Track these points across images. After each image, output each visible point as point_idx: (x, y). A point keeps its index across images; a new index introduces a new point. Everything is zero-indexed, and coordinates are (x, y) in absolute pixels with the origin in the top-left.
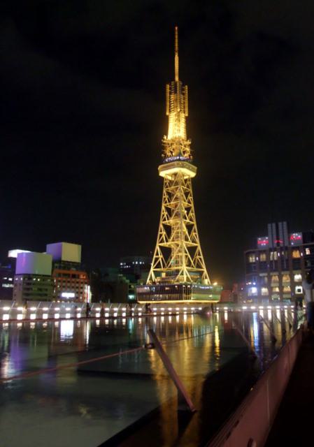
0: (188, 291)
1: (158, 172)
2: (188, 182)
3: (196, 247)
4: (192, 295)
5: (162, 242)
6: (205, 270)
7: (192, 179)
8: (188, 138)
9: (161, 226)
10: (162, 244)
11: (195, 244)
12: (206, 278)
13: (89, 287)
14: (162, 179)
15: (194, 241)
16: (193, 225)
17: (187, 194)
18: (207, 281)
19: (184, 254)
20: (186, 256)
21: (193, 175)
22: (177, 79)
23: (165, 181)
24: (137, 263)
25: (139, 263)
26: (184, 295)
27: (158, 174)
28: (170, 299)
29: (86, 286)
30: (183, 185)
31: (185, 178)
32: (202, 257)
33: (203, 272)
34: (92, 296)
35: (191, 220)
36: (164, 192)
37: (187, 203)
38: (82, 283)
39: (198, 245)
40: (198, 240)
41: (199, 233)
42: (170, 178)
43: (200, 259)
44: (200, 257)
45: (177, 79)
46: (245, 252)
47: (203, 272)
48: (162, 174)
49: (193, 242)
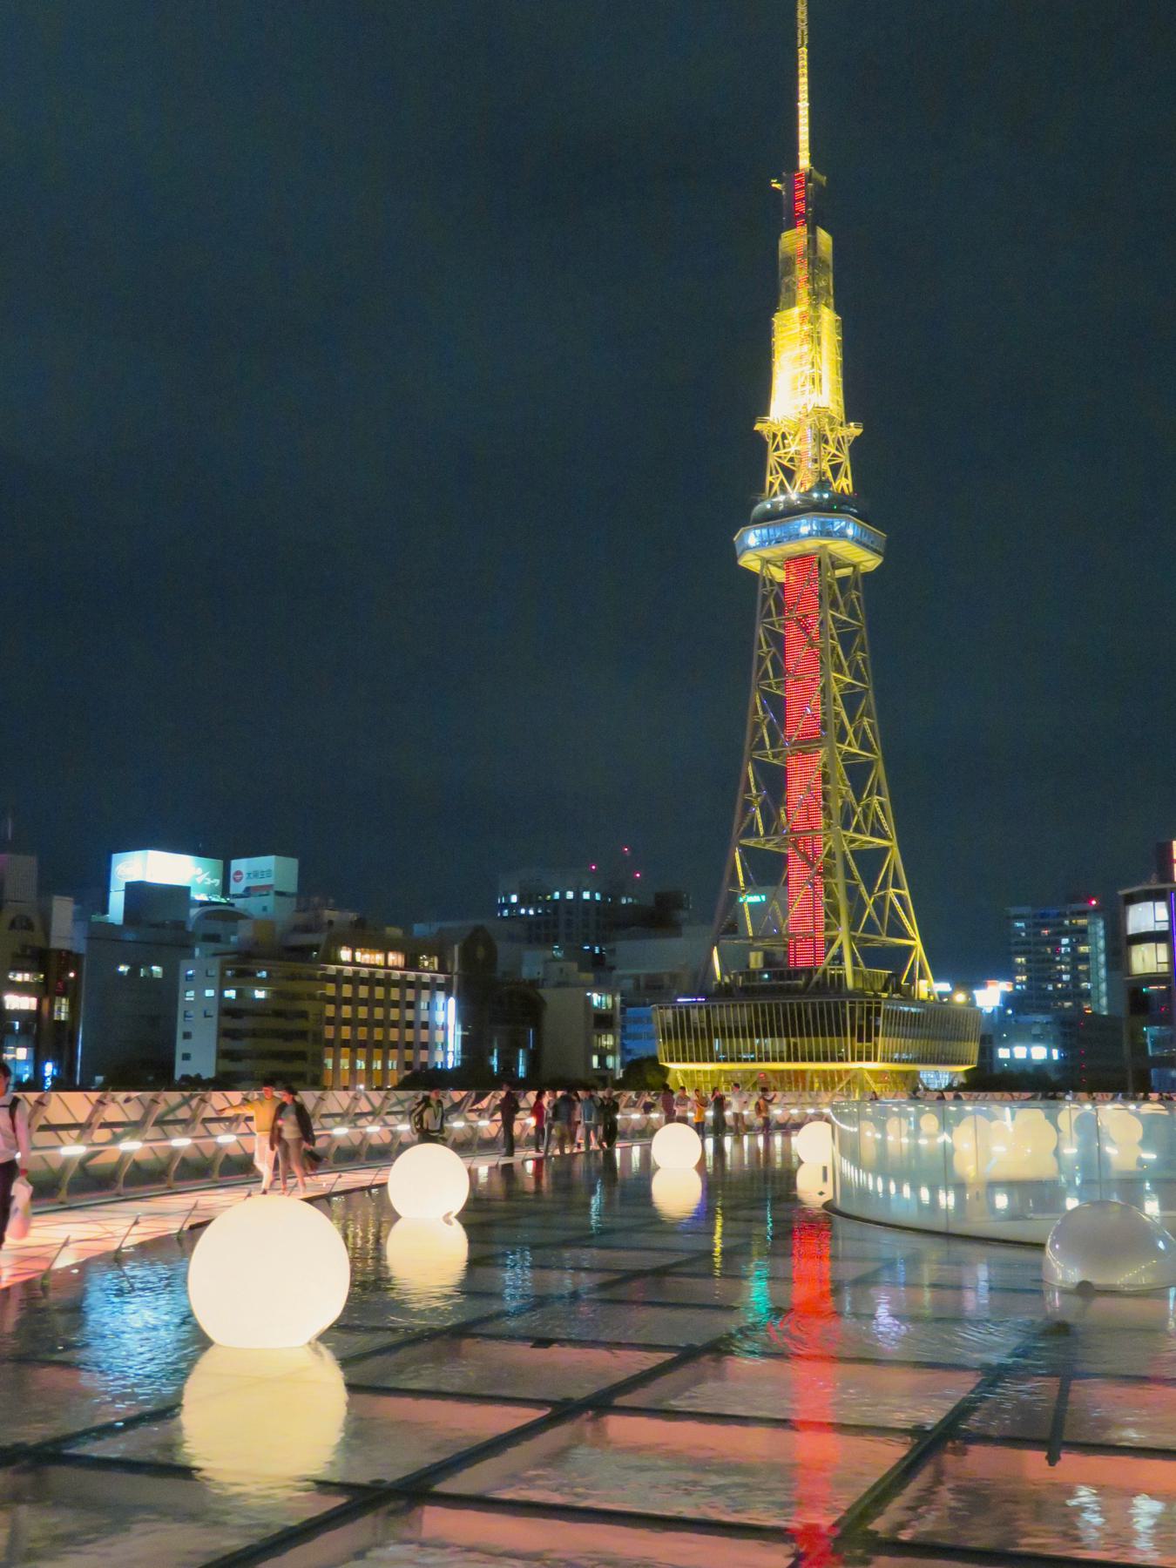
3: (886, 850)
5: (751, 831)
6: (917, 943)
7: (866, 575)
8: (851, 413)
10: (751, 842)
11: (885, 843)
12: (922, 976)
13: (452, 1001)
14: (751, 577)
16: (869, 766)
17: (846, 640)
20: (852, 892)
21: (870, 561)
22: (804, 162)
23: (761, 591)
24: (586, 895)
25: (592, 896)
27: (735, 559)
28: (793, 1056)
29: (440, 997)
30: (834, 604)
31: (840, 573)
32: (906, 893)
33: (908, 950)
34: (463, 1037)
35: (865, 745)
36: (760, 632)
38: (426, 986)
39: (892, 844)
40: (888, 826)
41: (892, 799)
42: (779, 575)
43: (899, 897)
44: (898, 894)
45: (804, 162)
46: (1122, 893)
47: (908, 950)
48: (750, 562)
49: (872, 835)
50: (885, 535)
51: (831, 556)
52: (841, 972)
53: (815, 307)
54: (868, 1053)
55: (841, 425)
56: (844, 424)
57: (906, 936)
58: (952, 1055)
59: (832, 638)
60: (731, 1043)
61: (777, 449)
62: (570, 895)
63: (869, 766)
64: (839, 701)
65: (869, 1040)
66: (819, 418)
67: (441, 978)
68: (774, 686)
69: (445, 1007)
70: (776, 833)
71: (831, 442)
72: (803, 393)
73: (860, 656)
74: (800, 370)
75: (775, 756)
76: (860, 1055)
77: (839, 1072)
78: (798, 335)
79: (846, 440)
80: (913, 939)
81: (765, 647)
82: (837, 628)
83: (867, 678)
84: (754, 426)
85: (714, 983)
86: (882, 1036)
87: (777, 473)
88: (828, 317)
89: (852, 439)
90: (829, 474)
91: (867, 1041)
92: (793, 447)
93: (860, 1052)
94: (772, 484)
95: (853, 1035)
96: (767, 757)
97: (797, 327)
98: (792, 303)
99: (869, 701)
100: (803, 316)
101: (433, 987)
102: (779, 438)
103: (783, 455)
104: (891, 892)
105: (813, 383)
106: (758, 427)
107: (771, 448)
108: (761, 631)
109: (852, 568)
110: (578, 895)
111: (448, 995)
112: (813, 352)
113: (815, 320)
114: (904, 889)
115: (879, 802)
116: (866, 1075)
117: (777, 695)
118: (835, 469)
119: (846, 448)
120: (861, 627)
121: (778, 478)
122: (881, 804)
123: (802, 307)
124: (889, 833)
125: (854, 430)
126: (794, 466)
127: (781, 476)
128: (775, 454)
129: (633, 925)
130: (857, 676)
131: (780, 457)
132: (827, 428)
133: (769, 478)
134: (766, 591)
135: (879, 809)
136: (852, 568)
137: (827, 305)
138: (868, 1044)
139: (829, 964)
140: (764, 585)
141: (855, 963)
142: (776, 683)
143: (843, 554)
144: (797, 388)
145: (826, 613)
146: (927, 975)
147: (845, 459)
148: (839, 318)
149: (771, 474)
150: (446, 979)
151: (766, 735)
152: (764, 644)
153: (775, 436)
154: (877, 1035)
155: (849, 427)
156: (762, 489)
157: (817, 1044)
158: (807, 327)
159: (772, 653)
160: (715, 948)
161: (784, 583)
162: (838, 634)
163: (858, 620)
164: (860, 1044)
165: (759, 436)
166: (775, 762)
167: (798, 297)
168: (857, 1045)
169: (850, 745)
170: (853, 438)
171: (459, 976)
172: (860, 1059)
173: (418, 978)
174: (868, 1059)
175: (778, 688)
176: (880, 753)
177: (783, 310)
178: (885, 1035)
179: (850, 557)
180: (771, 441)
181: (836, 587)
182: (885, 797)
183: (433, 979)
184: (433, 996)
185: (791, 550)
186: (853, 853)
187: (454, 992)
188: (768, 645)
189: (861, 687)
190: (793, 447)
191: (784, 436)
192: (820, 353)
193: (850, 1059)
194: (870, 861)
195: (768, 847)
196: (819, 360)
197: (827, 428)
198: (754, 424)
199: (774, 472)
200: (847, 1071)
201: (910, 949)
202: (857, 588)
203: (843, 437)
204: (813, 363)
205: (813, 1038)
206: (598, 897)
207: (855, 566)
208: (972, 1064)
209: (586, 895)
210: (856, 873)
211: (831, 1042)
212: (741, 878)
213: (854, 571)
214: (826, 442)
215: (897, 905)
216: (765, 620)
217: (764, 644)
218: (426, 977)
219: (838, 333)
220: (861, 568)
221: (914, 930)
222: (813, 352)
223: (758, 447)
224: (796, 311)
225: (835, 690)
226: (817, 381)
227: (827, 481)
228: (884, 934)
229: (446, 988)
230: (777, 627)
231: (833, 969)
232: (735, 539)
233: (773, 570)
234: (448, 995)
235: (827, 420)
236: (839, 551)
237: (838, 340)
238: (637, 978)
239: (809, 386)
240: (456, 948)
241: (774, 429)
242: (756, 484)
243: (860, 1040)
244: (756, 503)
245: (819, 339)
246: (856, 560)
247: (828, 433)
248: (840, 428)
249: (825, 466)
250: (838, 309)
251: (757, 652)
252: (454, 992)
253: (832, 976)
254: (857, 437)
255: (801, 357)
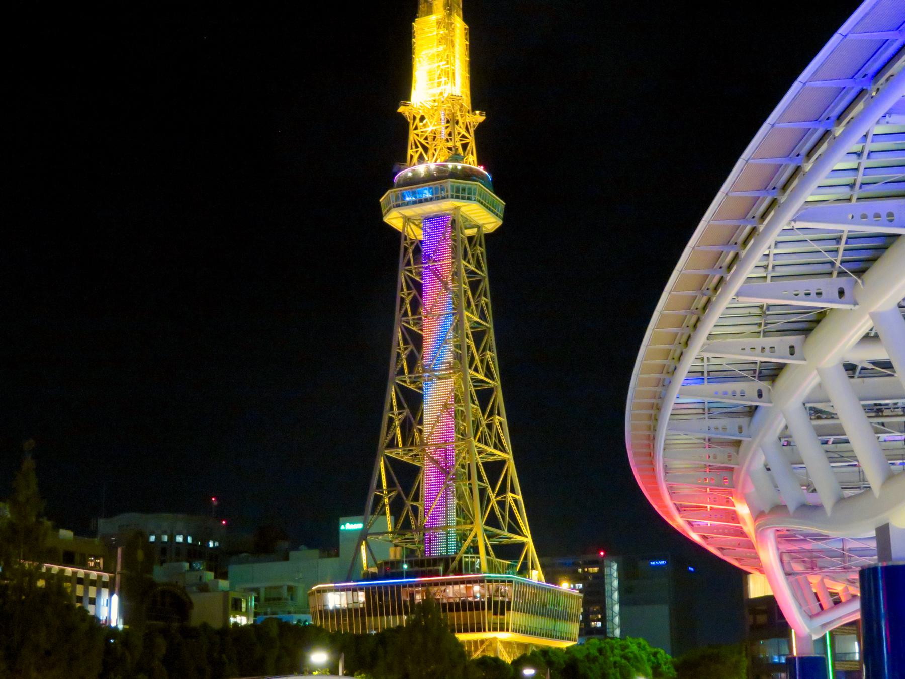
0: (500, 608)
1: (378, 214)
2: (480, 250)
4: (513, 617)
5: (392, 444)
6: (527, 539)
7: (487, 236)
8: (477, 103)
9: (392, 393)
10: (392, 453)
11: (504, 456)
12: (533, 568)
13: (115, 598)
14: (394, 236)
15: (499, 445)
16: (490, 391)
17: (474, 286)
18: (536, 576)
19: (476, 484)
20: (482, 491)
23: (403, 244)
24: (179, 539)
25: (185, 539)
26: (488, 616)
29: (105, 593)
31: (469, 232)
32: (520, 498)
35: (489, 374)
37: (476, 319)
38: (93, 583)
43: (516, 501)
44: (515, 497)
48: (394, 219)
49: (495, 447)
50: (504, 203)
51: (461, 216)
52: (473, 560)
53: (450, 15)
54: (502, 624)
55: (468, 112)
56: (470, 112)
57: (519, 532)
58: (561, 632)
59: (465, 284)
60: (376, 621)
61: (416, 128)
62: (166, 538)
63: (490, 391)
64: (470, 336)
65: (503, 613)
66: (453, 105)
67: (106, 577)
68: (411, 323)
69: (109, 603)
70: (412, 444)
71: (460, 123)
72: (439, 84)
73: (483, 300)
74: (436, 65)
75: (413, 383)
76: (495, 626)
77: (475, 642)
78: (436, 37)
79: (472, 125)
80: (527, 537)
81: (405, 290)
82: (468, 277)
83: (489, 319)
84: (397, 109)
85: (362, 572)
86: (513, 610)
87: (417, 147)
88: (459, 25)
89: (476, 124)
90: (460, 151)
91: (500, 615)
92: (430, 126)
93: (495, 623)
94: (412, 157)
95: (489, 609)
96: (405, 382)
97: (435, 31)
98: (430, 12)
99: (491, 337)
100: (439, 23)
101: (99, 584)
102: (417, 120)
103: (420, 134)
104: (510, 495)
105: (448, 77)
106: (401, 109)
107: (412, 127)
108: (403, 277)
109: (475, 230)
110: (172, 538)
111: (111, 594)
112: (448, 51)
113: (450, 25)
114: (518, 495)
115: (500, 420)
116: (499, 643)
117: (413, 331)
118: (464, 147)
119: (472, 130)
120: (484, 278)
121: (417, 152)
122: (501, 424)
123: (438, 14)
124: (507, 448)
125: (479, 118)
126: (428, 143)
127: (421, 150)
128: (415, 132)
129: (246, 552)
130: (483, 316)
131: (418, 135)
132: (458, 113)
133: (410, 152)
134: (407, 244)
135: (499, 427)
136: (475, 230)
137: (458, 15)
138: (502, 617)
139: (466, 553)
140: (406, 239)
141: (488, 553)
142: (414, 319)
143: (472, 216)
144: (434, 79)
145: (459, 261)
146: (537, 566)
147: (471, 140)
148: (467, 27)
149: (412, 149)
150: (110, 578)
151: (405, 364)
152: (404, 287)
153: (415, 118)
154: (509, 609)
155: (475, 114)
156: (404, 160)
157: (459, 618)
158: (443, 31)
159: (412, 295)
160: (364, 542)
161: (423, 241)
162: (469, 282)
163: (482, 271)
164: (495, 616)
165: (401, 115)
166: (412, 387)
167: (435, 7)
168: (493, 617)
169: (476, 370)
170: (478, 123)
171: (121, 574)
172: (495, 630)
173: (87, 575)
174: (502, 630)
175: (415, 325)
176: (499, 382)
177: (422, 16)
178: (515, 610)
179: (475, 219)
180: (412, 121)
181: (466, 242)
182: (504, 418)
183: (99, 577)
184: (98, 593)
185: (430, 210)
186: (484, 464)
187: (117, 589)
188: (409, 288)
189: (486, 327)
190: (430, 126)
191: (422, 118)
192: (453, 53)
193: (487, 629)
194: (494, 469)
195: (405, 459)
196: (452, 58)
197: (458, 113)
198: (398, 107)
199: (414, 147)
200: (482, 642)
201: (522, 545)
202: (480, 246)
203: (469, 123)
204: (448, 63)
205: (461, 612)
206: (189, 540)
207: (479, 227)
208: (575, 641)
209: (179, 539)
210: (485, 478)
211: (476, 614)
212: (384, 484)
213: (478, 231)
214: (457, 123)
215: (515, 508)
216: (407, 268)
217: (404, 287)
218: (94, 575)
219: (466, 39)
220: (484, 229)
221: (528, 532)
222: (448, 51)
223: (402, 126)
224: (433, 18)
225: (467, 325)
226: (451, 75)
227: (459, 155)
228: (506, 530)
229: (110, 587)
230: (415, 274)
231: (467, 557)
232: (381, 200)
233: (413, 226)
234: (111, 594)
235: (459, 107)
236: (467, 213)
237: (466, 44)
238: (256, 590)
239: (444, 79)
240: (119, 551)
241: (414, 112)
242: (401, 157)
243: (495, 613)
244: (399, 171)
245: (452, 41)
246: (480, 222)
247: (459, 118)
248: (467, 114)
249: (458, 144)
250: (466, 19)
251: (400, 295)
252: (117, 589)
253: (467, 563)
254: (480, 123)
255: (438, 55)
